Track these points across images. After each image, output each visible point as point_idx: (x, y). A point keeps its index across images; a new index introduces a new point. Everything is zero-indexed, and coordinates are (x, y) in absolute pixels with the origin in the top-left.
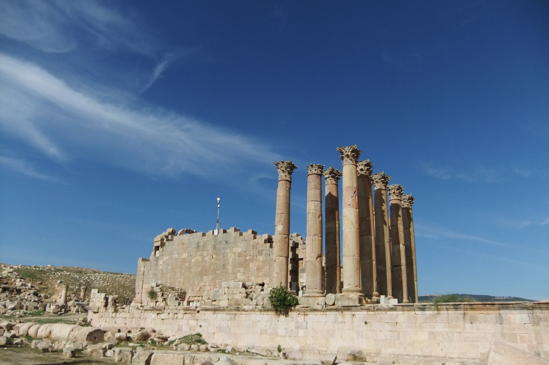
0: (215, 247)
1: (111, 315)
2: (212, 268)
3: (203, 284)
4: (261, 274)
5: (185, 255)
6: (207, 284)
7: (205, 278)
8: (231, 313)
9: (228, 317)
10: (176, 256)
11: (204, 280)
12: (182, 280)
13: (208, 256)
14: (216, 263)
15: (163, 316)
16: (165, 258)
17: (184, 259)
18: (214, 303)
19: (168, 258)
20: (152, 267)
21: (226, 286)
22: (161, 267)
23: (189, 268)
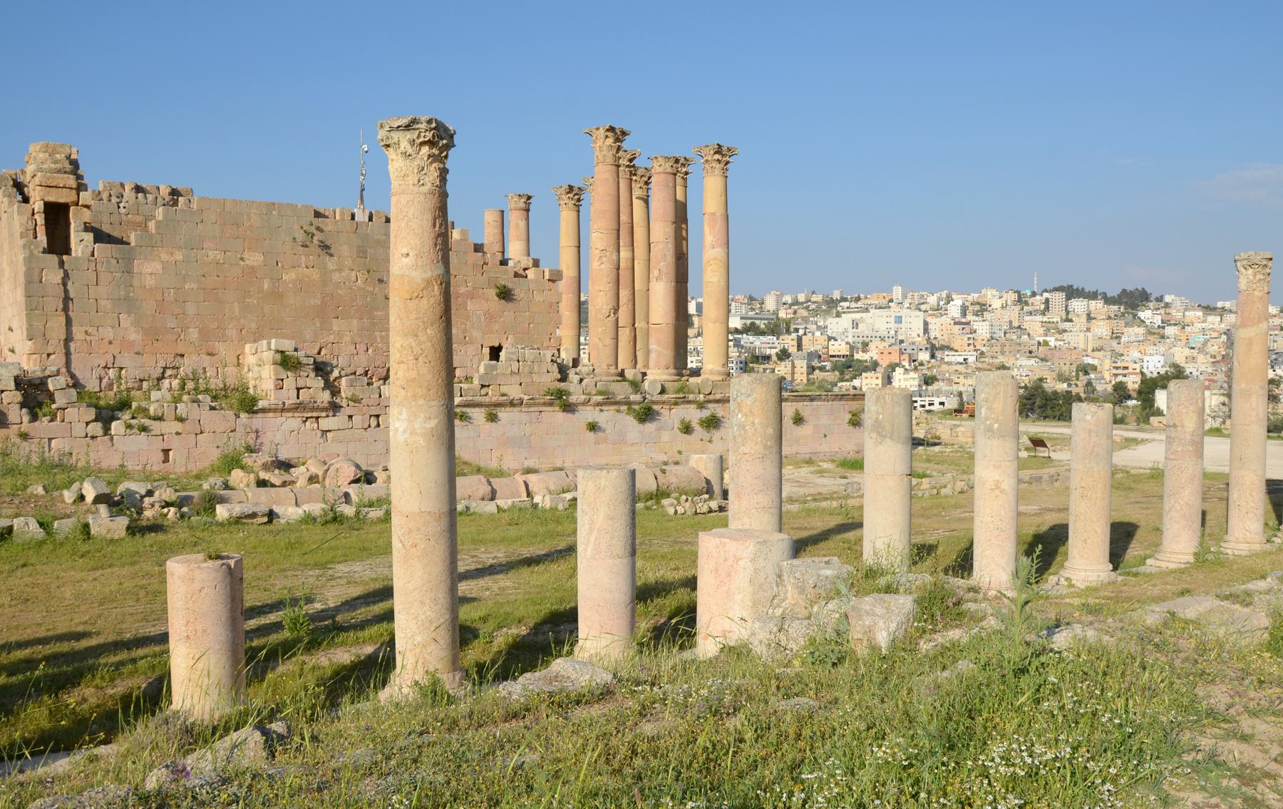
0: (362, 252)
1: (79, 429)
2: (359, 302)
3: (331, 338)
4: (496, 327)
5: (254, 259)
6: (347, 339)
7: (336, 325)
8: (532, 409)
9: (524, 417)
10: (220, 257)
11: (335, 328)
12: (253, 325)
13: (340, 270)
14: (372, 293)
15: (326, 423)
16: (164, 257)
17: (253, 268)
18: (484, 391)
19: (179, 256)
20: (104, 277)
21: (515, 357)
22: (150, 282)
23: (276, 295)
